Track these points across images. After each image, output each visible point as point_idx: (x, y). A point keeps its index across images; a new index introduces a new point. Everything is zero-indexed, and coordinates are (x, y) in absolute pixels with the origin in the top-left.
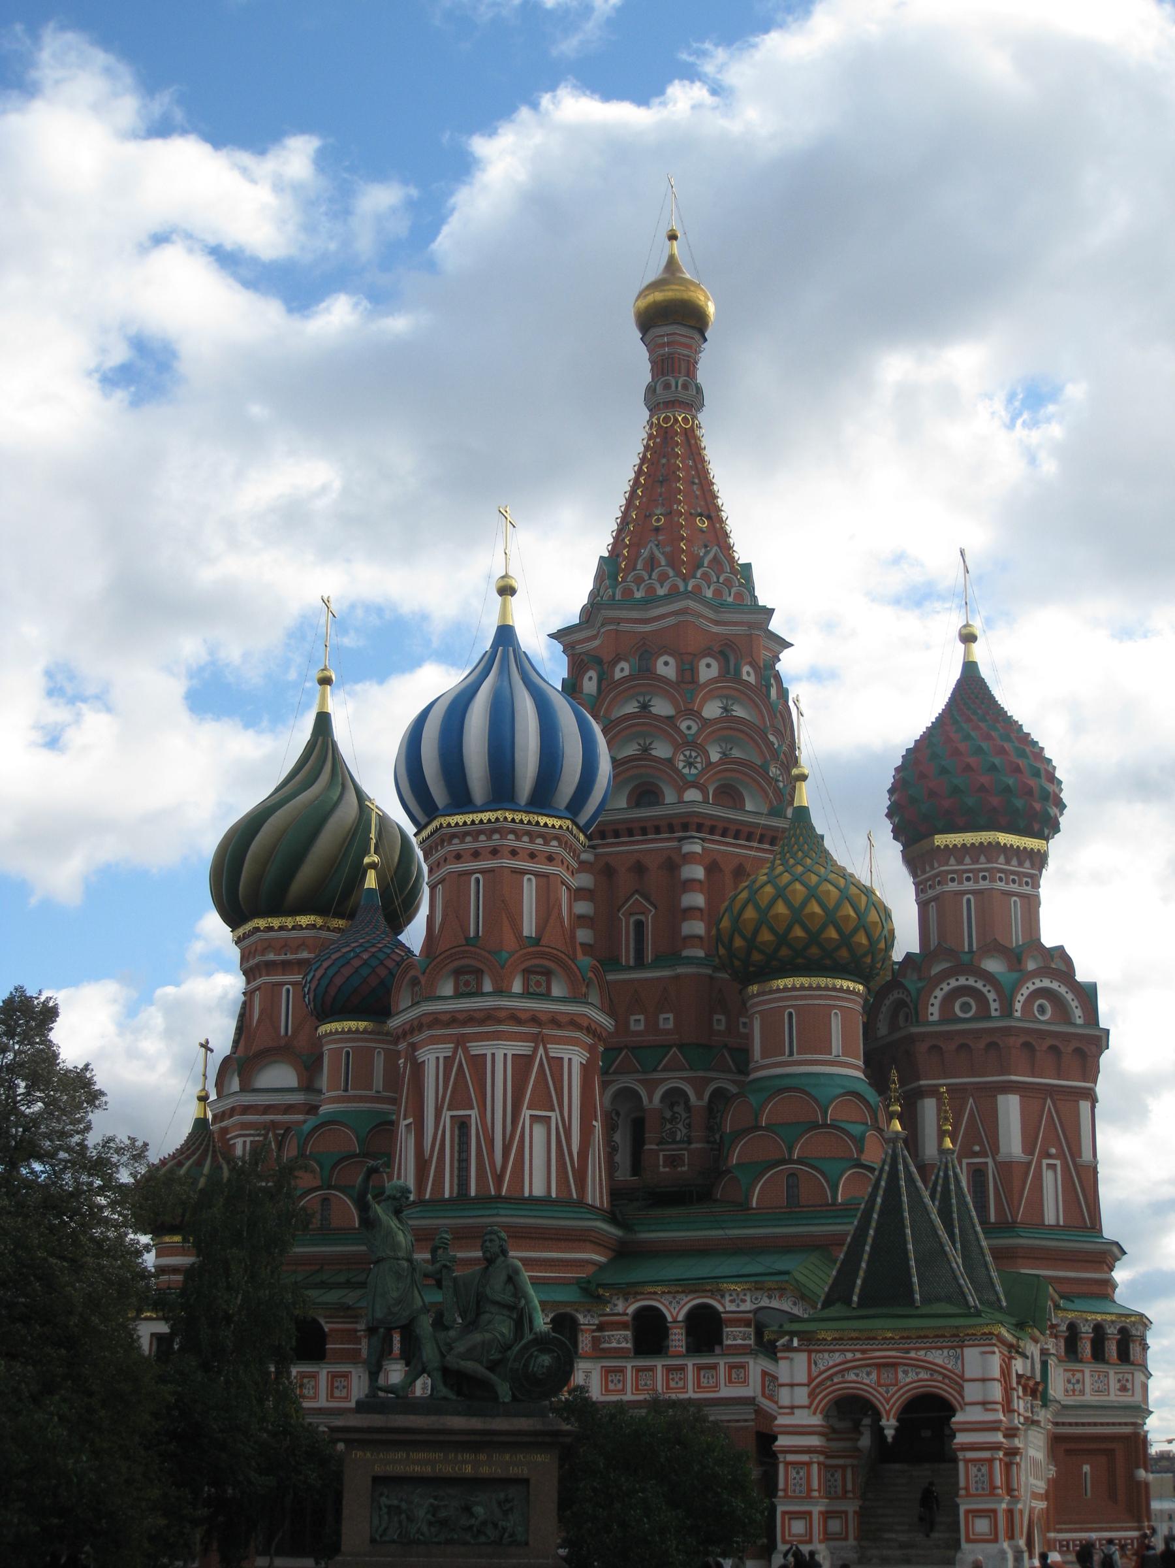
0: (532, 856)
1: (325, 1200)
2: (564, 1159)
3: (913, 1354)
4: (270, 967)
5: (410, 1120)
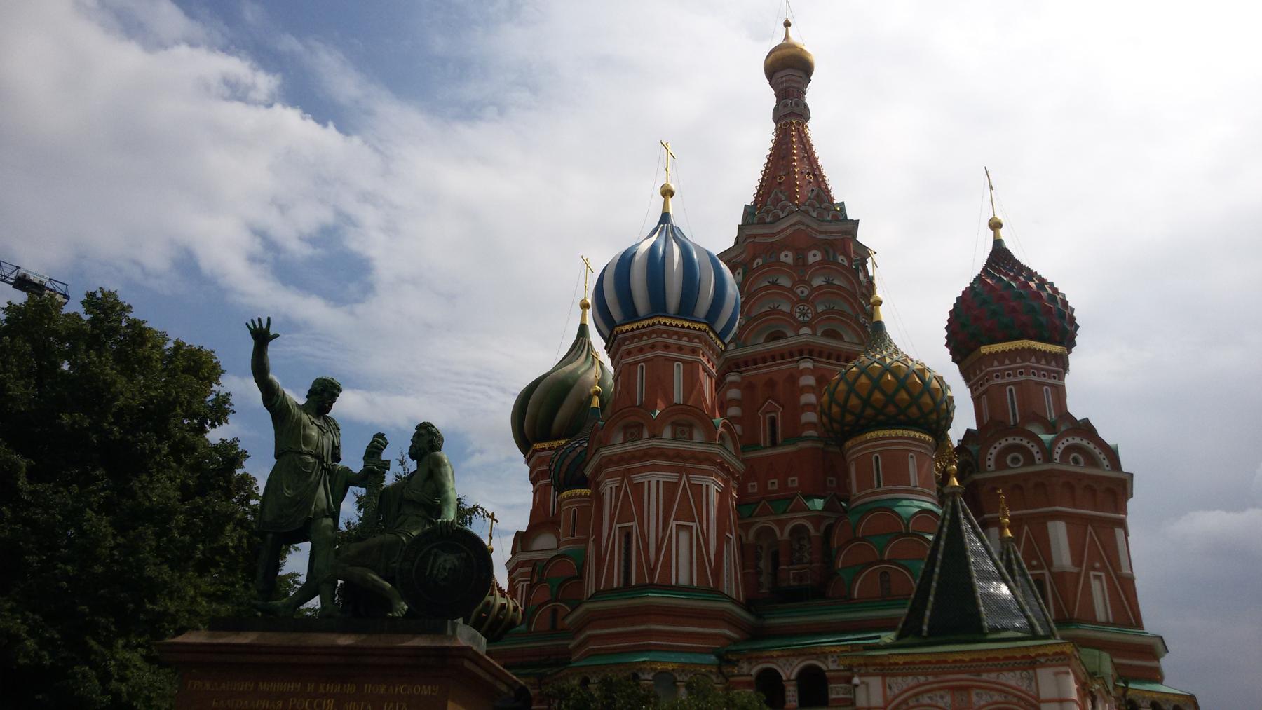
0: (680, 349)
1: (555, 612)
2: (703, 557)
3: (985, 676)
4: (543, 474)
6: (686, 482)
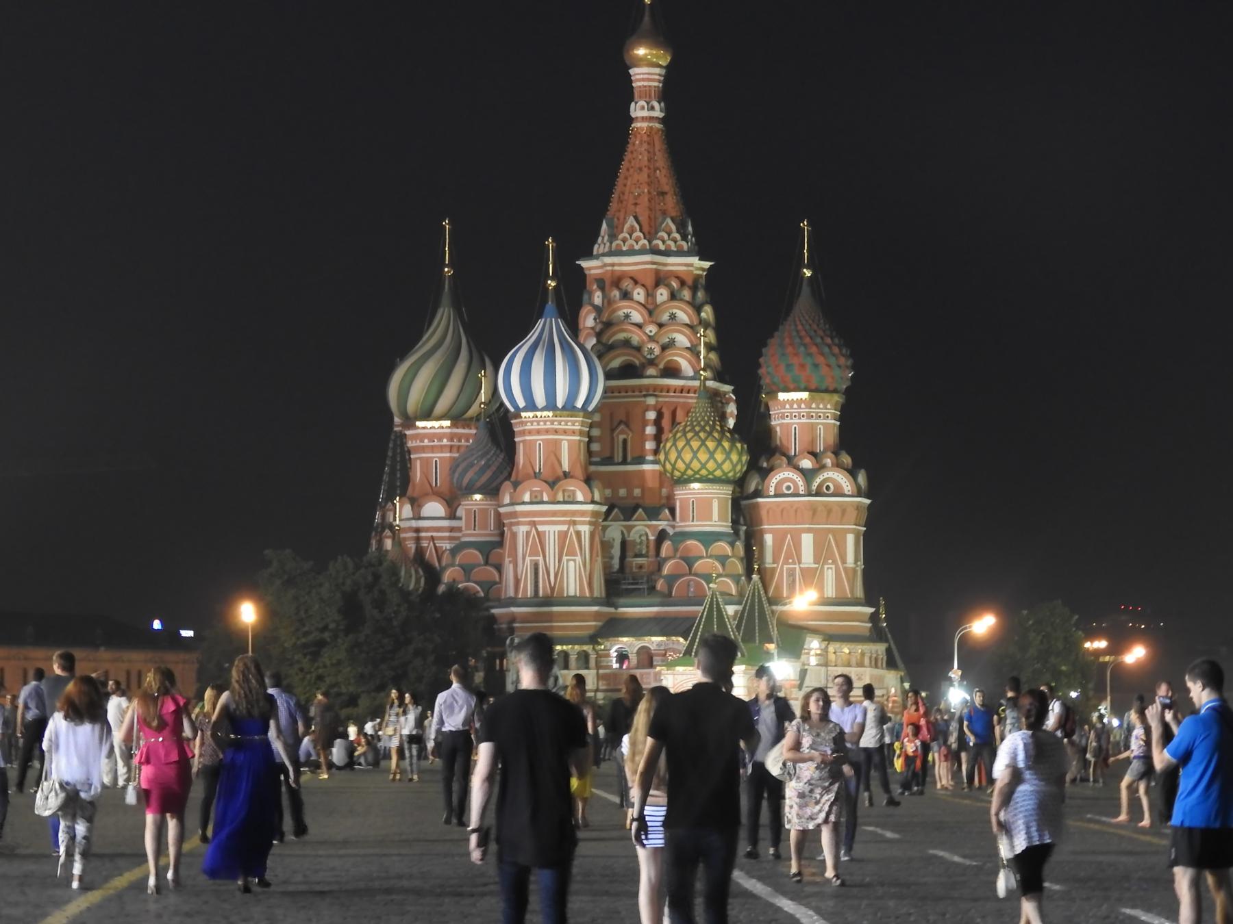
0: (565, 432)
5: (510, 559)
6: (573, 533)
